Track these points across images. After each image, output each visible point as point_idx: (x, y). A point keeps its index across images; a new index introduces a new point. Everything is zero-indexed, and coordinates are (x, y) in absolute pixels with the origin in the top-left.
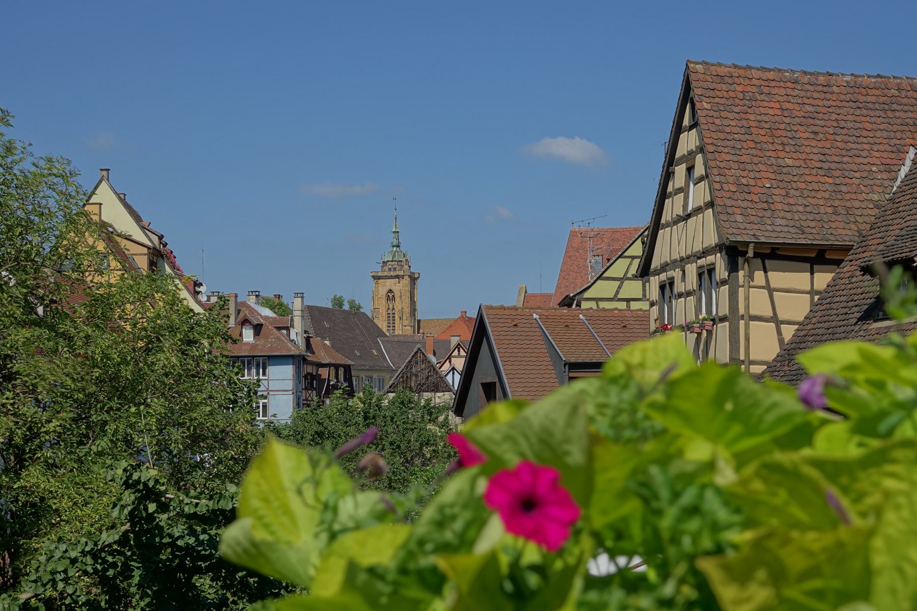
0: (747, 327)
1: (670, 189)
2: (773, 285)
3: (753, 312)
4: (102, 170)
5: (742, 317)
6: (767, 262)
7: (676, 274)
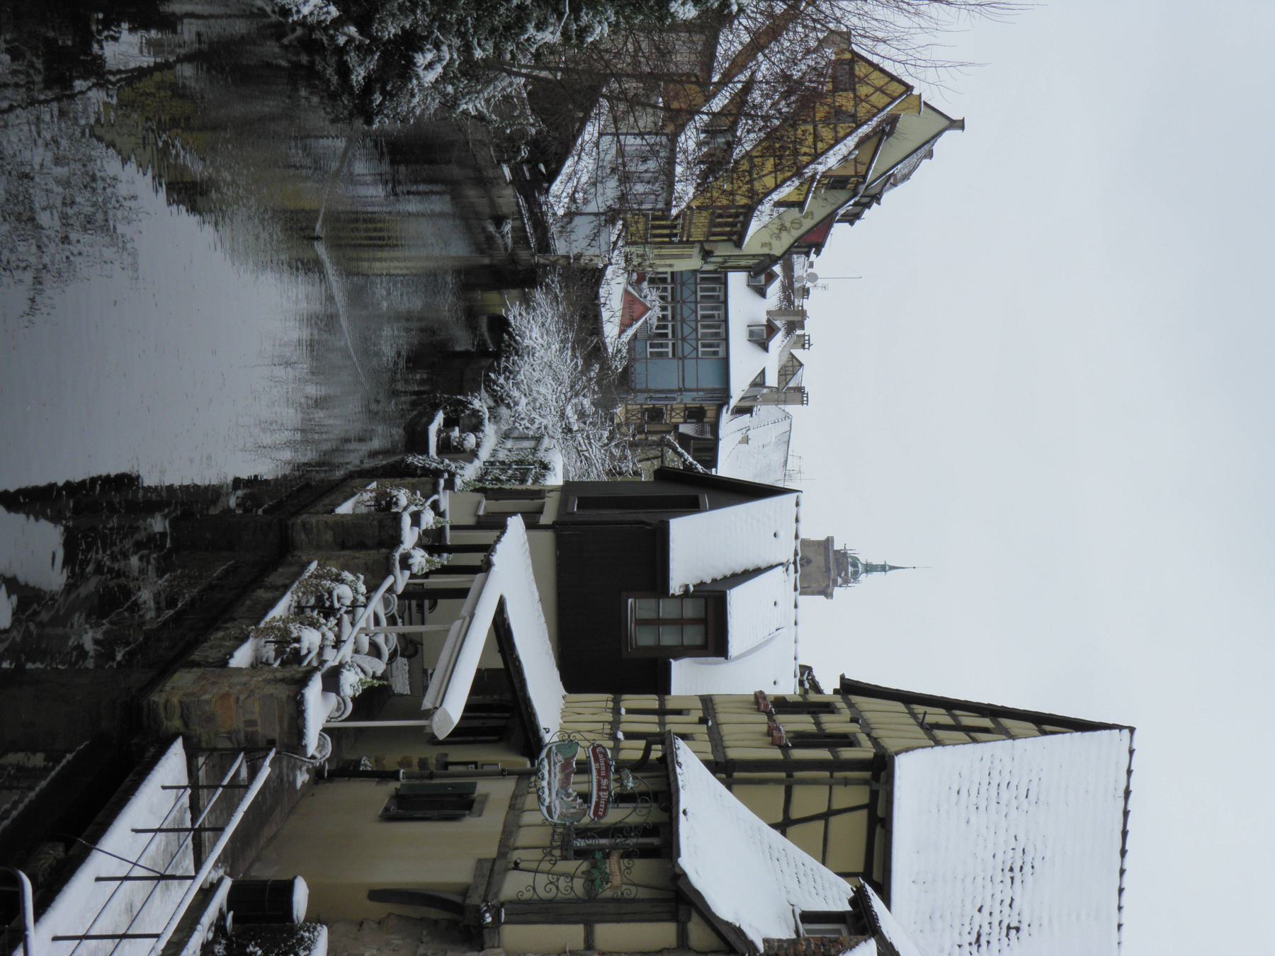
0: (777, 782)
1: (957, 712)
2: (834, 820)
3: (798, 791)
4: (963, 120)
5: (790, 776)
6: (863, 814)
7: (846, 714)
